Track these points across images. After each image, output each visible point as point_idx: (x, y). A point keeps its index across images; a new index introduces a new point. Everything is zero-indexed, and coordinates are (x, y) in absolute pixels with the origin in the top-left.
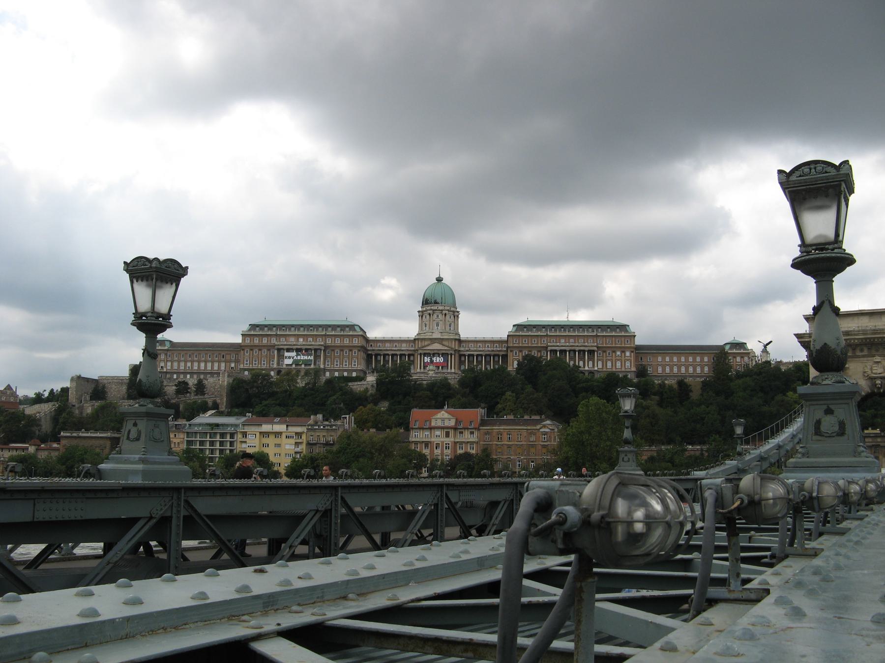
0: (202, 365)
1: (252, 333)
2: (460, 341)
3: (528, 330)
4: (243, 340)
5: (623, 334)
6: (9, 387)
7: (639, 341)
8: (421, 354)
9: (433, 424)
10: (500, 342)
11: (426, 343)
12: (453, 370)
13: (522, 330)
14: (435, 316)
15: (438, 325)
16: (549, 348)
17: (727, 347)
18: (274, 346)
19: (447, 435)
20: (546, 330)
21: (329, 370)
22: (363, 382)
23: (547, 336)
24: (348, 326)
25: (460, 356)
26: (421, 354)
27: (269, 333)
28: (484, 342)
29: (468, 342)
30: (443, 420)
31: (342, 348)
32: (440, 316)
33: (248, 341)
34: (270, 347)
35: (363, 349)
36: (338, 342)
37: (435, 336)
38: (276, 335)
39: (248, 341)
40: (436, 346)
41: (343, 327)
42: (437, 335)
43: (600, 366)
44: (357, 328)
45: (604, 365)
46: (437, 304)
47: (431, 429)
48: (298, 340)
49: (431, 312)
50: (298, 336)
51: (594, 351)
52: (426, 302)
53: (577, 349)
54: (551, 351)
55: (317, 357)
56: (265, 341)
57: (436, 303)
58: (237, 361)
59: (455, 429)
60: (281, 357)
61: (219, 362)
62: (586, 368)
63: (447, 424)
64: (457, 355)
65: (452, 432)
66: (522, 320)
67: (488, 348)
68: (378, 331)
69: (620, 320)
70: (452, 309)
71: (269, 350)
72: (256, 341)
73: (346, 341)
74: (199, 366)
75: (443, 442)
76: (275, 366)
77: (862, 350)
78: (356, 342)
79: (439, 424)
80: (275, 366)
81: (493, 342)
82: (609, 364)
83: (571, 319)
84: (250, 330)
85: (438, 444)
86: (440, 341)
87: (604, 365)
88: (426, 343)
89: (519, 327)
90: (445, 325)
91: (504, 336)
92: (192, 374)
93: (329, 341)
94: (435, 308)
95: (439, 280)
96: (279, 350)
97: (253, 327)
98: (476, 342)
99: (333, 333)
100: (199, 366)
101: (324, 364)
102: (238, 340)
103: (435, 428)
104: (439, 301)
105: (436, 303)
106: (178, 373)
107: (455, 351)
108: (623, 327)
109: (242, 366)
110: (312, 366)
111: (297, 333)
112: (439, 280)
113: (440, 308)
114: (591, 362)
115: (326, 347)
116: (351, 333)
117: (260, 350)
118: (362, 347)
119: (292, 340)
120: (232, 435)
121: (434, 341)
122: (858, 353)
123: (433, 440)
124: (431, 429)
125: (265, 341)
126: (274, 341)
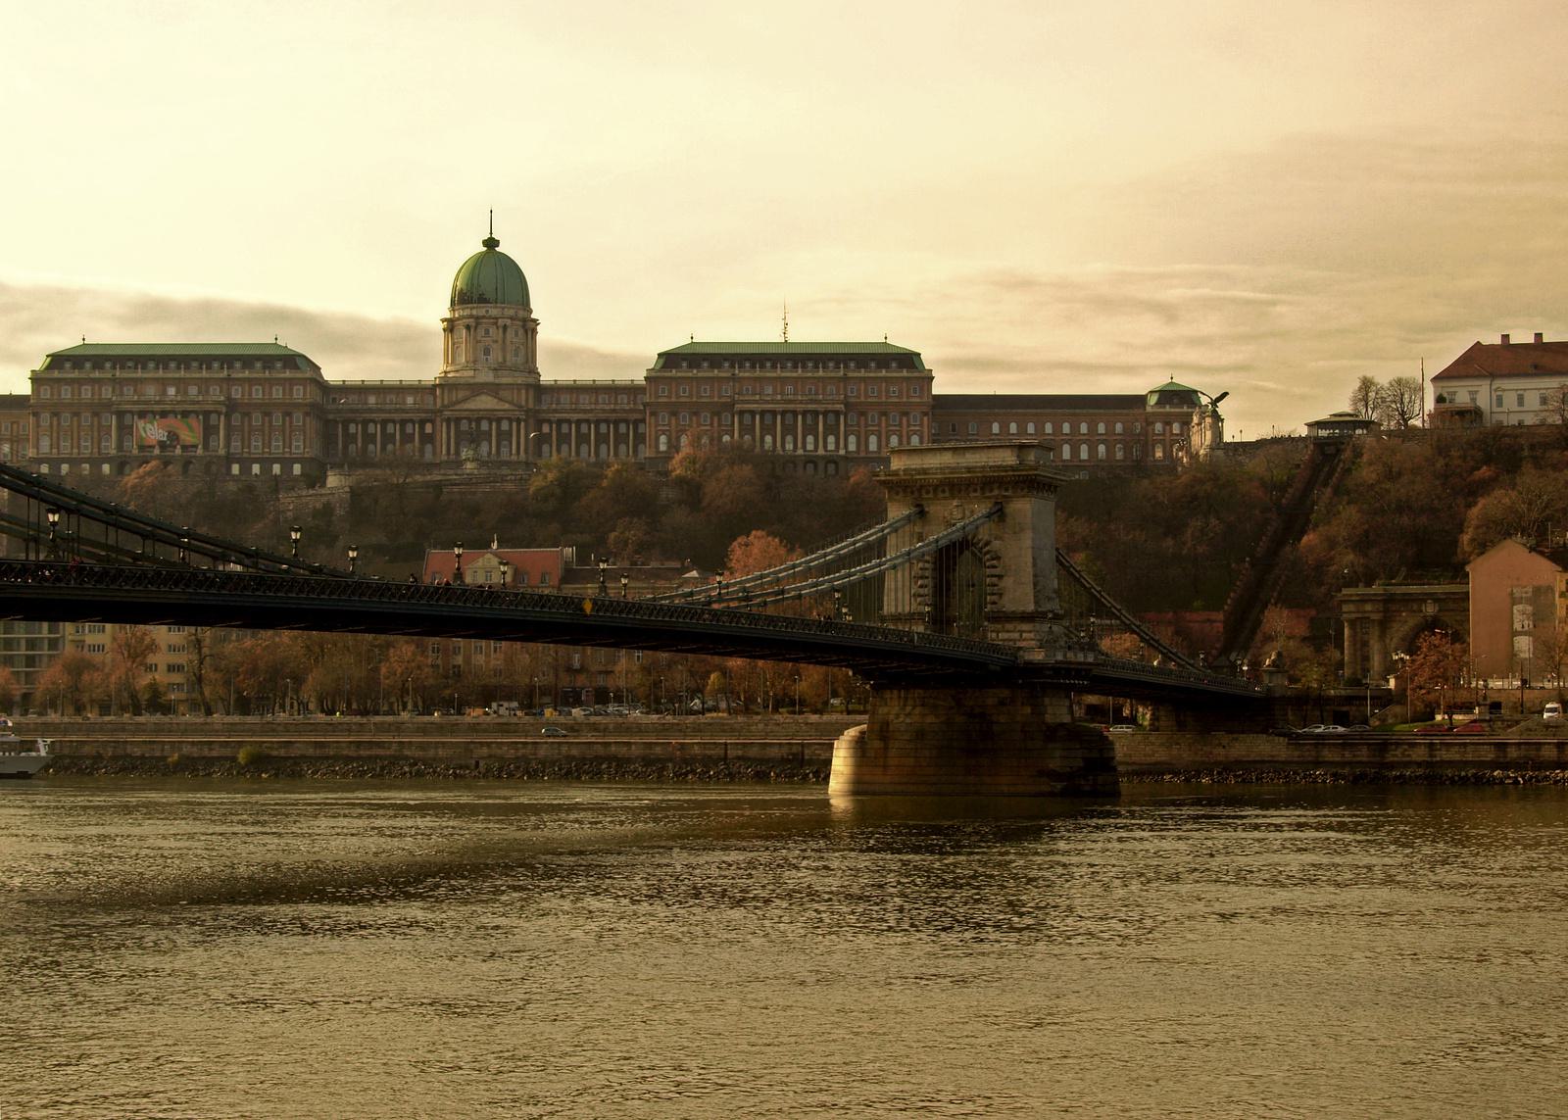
1: (56, 374)
2: (540, 390)
3: (690, 367)
5: (905, 373)
7: (939, 388)
8: (448, 421)
10: (631, 390)
11: (461, 394)
13: (677, 366)
14: (481, 332)
15: (487, 352)
16: (738, 407)
17: (1153, 400)
18: (108, 405)
20: (732, 366)
22: (319, 490)
23: (734, 378)
24: (279, 358)
26: (448, 421)
27: (97, 374)
28: (594, 389)
29: (557, 389)
31: (267, 409)
32: (492, 330)
33: (46, 393)
34: (99, 409)
35: (315, 410)
36: (258, 393)
38: (113, 380)
39: (46, 393)
40: (485, 402)
42: (485, 377)
43: (852, 447)
44: (299, 361)
45: (862, 442)
48: (164, 393)
49: (471, 321)
51: (837, 413)
53: (800, 407)
54: (741, 413)
55: (209, 431)
56: (87, 393)
57: (482, 300)
60: (125, 430)
62: (821, 452)
64: (531, 421)
67: (604, 403)
69: (903, 342)
70: (521, 314)
71: (96, 414)
72: (66, 394)
73: (277, 393)
76: (113, 452)
77: (943, 491)
78: (299, 394)
80: (113, 452)
81: (613, 390)
82: (873, 439)
83: (795, 337)
84: (49, 367)
86: (493, 389)
87: (862, 442)
88: (461, 394)
89: (669, 359)
90: (504, 350)
91: (639, 376)
93: (237, 393)
94: (482, 312)
95: (491, 243)
96: (120, 414)
97: (57, 360)
98: (576, 389)
99: (247, 374)
101: (228, 445)
102: (24, 388)
104: (489, 295)
107: (527, 411)
108: (909, 360)
110: (200, 451)
111: (161, 374)
112: (491, 243)
113: (494, 312)
114: (831, 439)
115: (232, 406)
116: (288, 374)
117: (77, 414)
118: (313, 405)
119: (151, 392)
121: (476, 389)
122: (941, 495)
125: (87, 393)
126: (107, 393)
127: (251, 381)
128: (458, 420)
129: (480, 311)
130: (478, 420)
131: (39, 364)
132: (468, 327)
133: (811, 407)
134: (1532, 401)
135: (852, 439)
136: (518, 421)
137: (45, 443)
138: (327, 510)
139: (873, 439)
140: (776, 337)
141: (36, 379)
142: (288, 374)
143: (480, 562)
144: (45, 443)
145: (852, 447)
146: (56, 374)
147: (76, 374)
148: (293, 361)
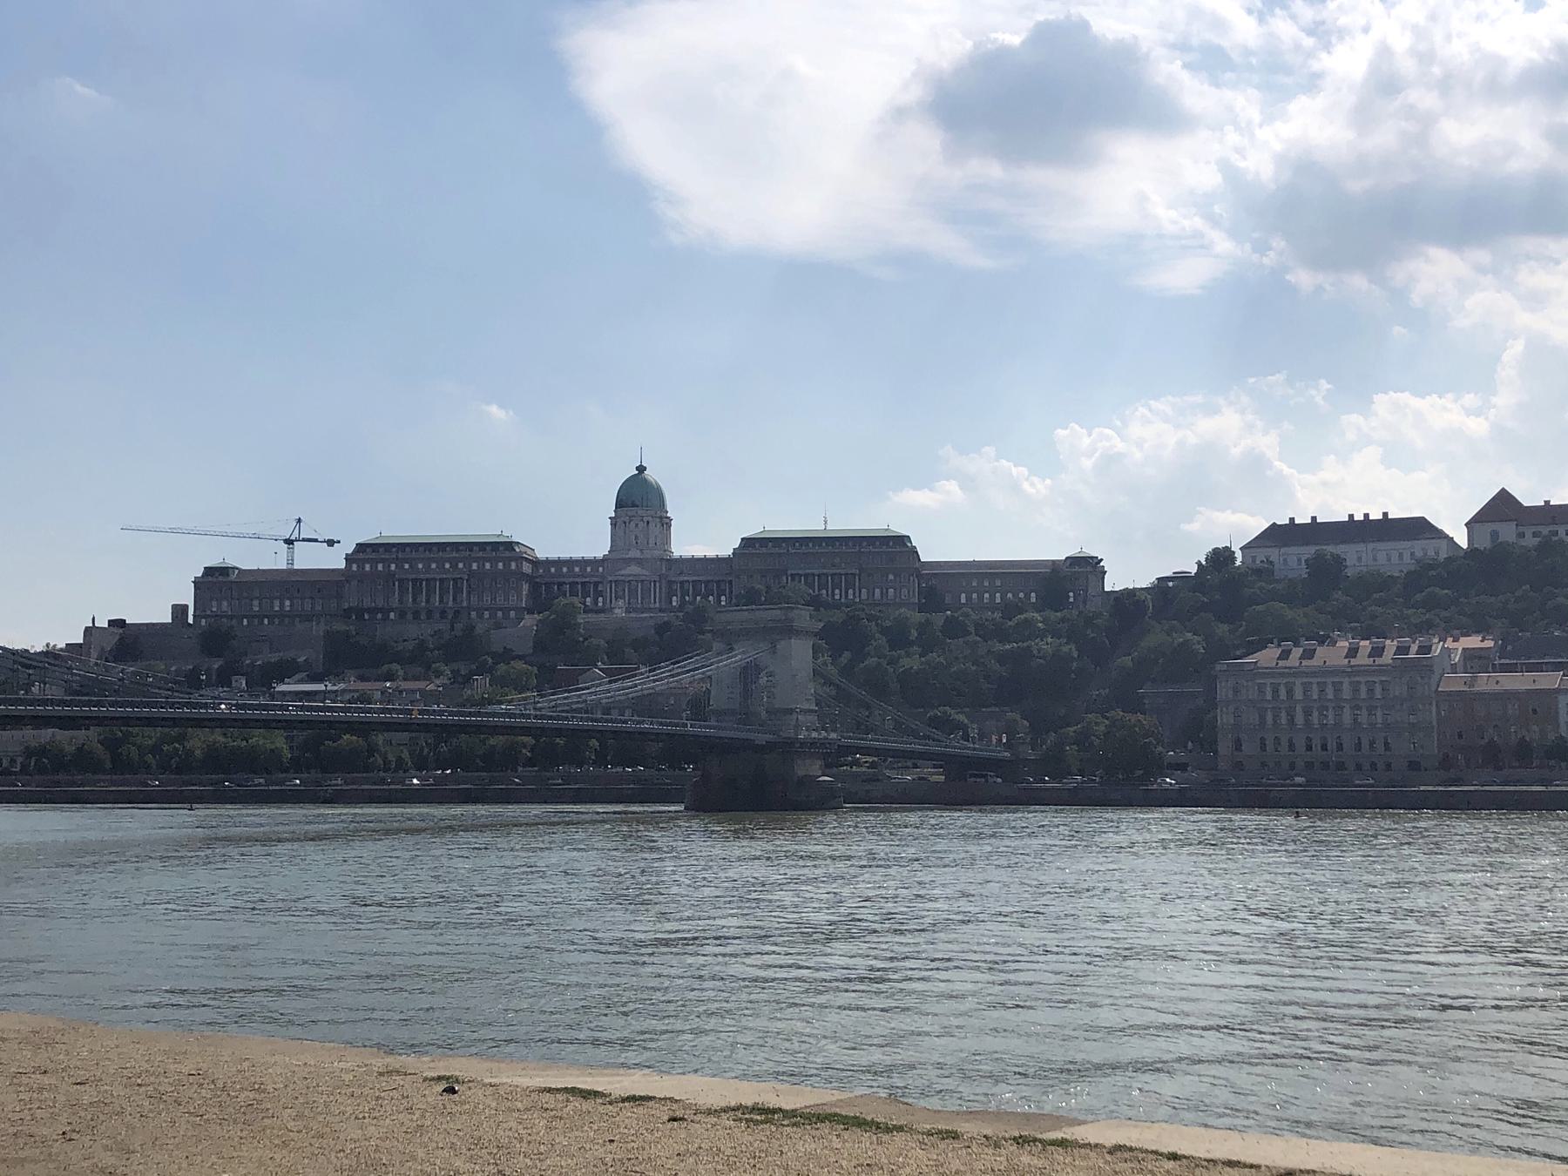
25: (670, 583)
29: (681, 560)
32: (641, 524)
37: (632, 554)
40: (634, 569)
41: (495, 546)
43: (864, 596)
46: (639, 503)
52: (619, 504)
74: (282, 605)
82: (877, 591)
86: (639, 562)
89: (747, 542)
95: (641, 469)
97: (361, 547)
100: (282, 605)
102: (342, 565)
112: (641, 469)
115: (471, 574)
129: (632, 511)
134: (1382, 558)
139: (877, 591)
141: (348, 558)
142: (507, 554)
145: (864, 596)
146: (361, 556)
148: (510, 545)
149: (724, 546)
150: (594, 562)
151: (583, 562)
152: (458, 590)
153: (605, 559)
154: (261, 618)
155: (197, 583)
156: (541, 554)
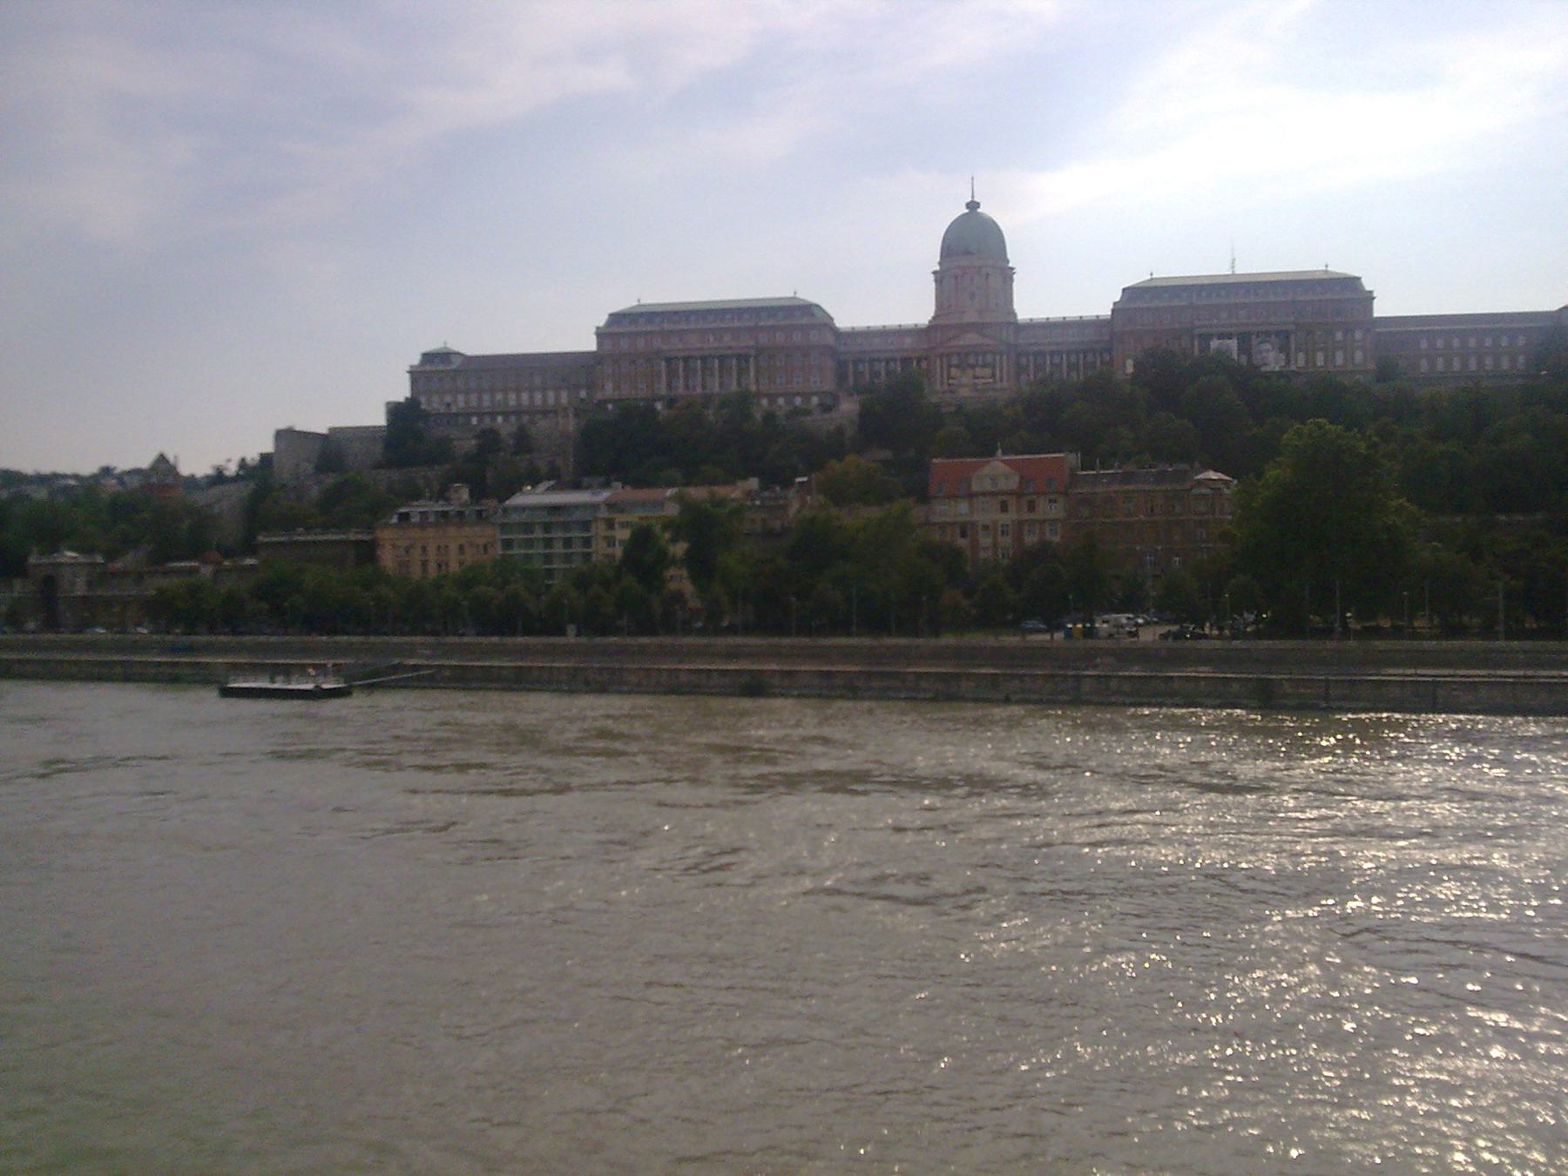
0: (525, 396)
1: (616, 329)
4: (600, 344)
6: (162, 459)
7: (1380, 310)
9: (975, 488)
10: (1097, 324)
12: (1005, 384)
16: (1197, 331)
19: (1004, 508)
21: (766, 395)
26: (941, 356)
27: (649, 328)
29: (1032, 326)
30: (994, 479)
40: (971, 339)
43: (1301, 363)
47: (971, 496)
50: (703, 332)
52: (947, 251)
57: (968, 253)
58: (591, 387)
59: (1018, 494)
61: (557, 389)
63: (1003, 485)
65: (1012, 502)
66: (1137, 276)
68: (853, 312)
69: (1341, 266)
72: (624, 344)
75: (995, 523)
76: (663, 391)
79: (988, 486)
85: (986, 527)
86: (979, 328)
92: (506, 415)
93: (763, 339)
95: (973, 206)
96: (669, 360)
97: (616, 318)
98: (1048, 326)
99: (771, 322)
102: (591, 345)
103: (975, 495)
105: (968, 253)
106: (481, 415)
108: (1352, 283)
109: (599, 396)
112: (973, 206)
116: (805, 321)
120: (586, 525)
121: (965, 328)
123: (975, 518)
124: (971, 496)
127: (773, 328)
128: (949, 355)
130: (967, 355)
131: (602, 321)
132: (956, 278)
133: (1264, 328)
135: (1301, 355)
136: (1001, 354)
137: (609, 386)
138: (840, 431)
140: (1225, 270)
141: (601, 335)
143: (987, 470)
144: (609, 386)
147: (633, 329)
149: (1093, 299)
150: (916, 332)
151: (900, 333)
152: (742, 372)
153: (932, 327)
154: (493, 415)
155: (416, 375)
156: (844, 320)
